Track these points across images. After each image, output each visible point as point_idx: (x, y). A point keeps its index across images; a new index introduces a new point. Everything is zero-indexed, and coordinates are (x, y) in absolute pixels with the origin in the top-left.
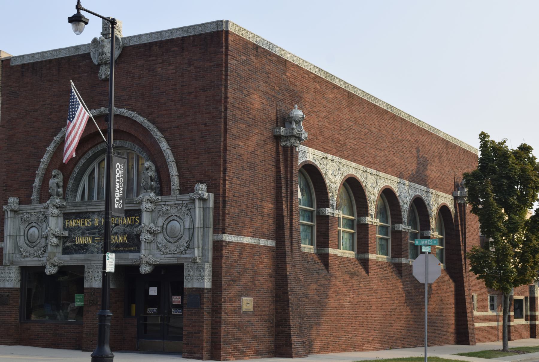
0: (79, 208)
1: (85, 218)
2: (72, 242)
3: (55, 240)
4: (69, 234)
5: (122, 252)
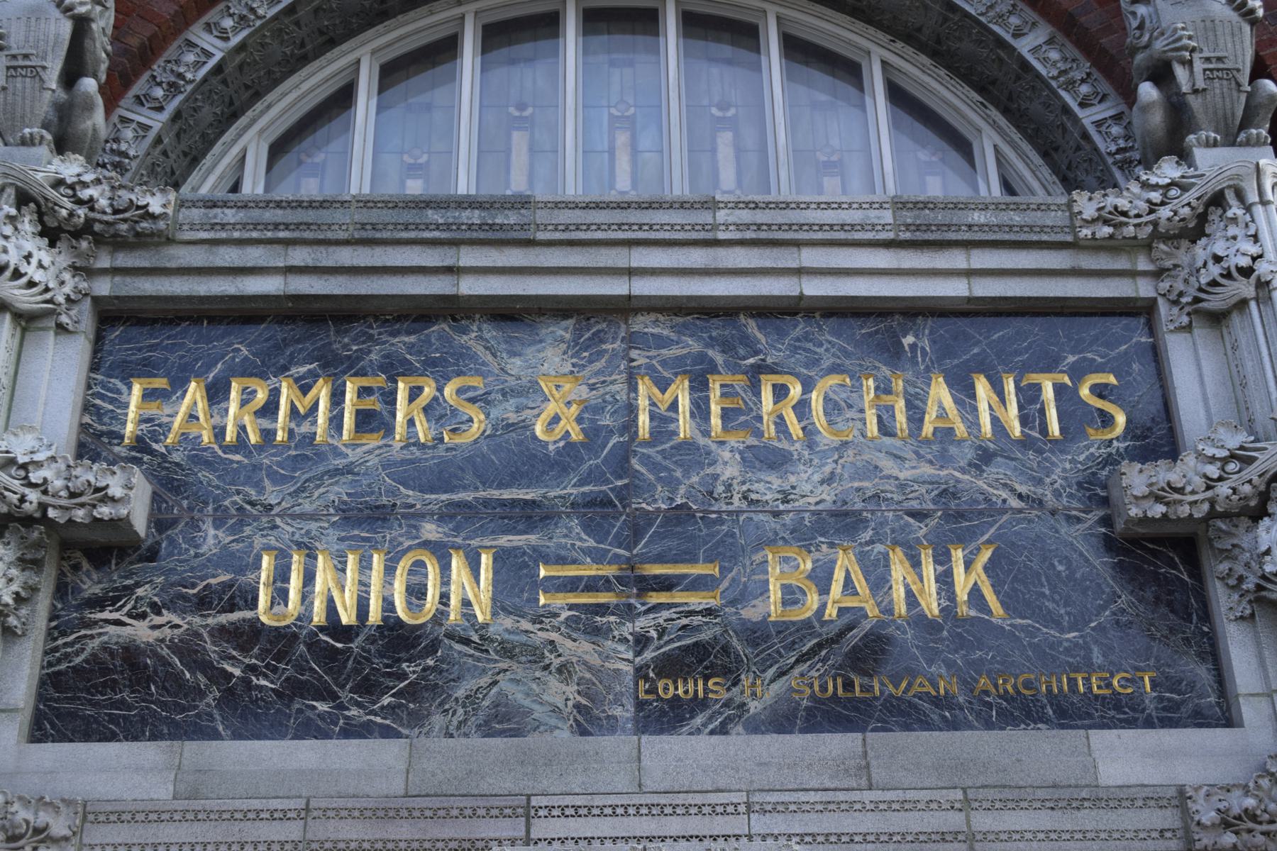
0: (346, 257)
1: (394, 368)
2: (203, 603)
4: (160, 523)
5: (954, 725)
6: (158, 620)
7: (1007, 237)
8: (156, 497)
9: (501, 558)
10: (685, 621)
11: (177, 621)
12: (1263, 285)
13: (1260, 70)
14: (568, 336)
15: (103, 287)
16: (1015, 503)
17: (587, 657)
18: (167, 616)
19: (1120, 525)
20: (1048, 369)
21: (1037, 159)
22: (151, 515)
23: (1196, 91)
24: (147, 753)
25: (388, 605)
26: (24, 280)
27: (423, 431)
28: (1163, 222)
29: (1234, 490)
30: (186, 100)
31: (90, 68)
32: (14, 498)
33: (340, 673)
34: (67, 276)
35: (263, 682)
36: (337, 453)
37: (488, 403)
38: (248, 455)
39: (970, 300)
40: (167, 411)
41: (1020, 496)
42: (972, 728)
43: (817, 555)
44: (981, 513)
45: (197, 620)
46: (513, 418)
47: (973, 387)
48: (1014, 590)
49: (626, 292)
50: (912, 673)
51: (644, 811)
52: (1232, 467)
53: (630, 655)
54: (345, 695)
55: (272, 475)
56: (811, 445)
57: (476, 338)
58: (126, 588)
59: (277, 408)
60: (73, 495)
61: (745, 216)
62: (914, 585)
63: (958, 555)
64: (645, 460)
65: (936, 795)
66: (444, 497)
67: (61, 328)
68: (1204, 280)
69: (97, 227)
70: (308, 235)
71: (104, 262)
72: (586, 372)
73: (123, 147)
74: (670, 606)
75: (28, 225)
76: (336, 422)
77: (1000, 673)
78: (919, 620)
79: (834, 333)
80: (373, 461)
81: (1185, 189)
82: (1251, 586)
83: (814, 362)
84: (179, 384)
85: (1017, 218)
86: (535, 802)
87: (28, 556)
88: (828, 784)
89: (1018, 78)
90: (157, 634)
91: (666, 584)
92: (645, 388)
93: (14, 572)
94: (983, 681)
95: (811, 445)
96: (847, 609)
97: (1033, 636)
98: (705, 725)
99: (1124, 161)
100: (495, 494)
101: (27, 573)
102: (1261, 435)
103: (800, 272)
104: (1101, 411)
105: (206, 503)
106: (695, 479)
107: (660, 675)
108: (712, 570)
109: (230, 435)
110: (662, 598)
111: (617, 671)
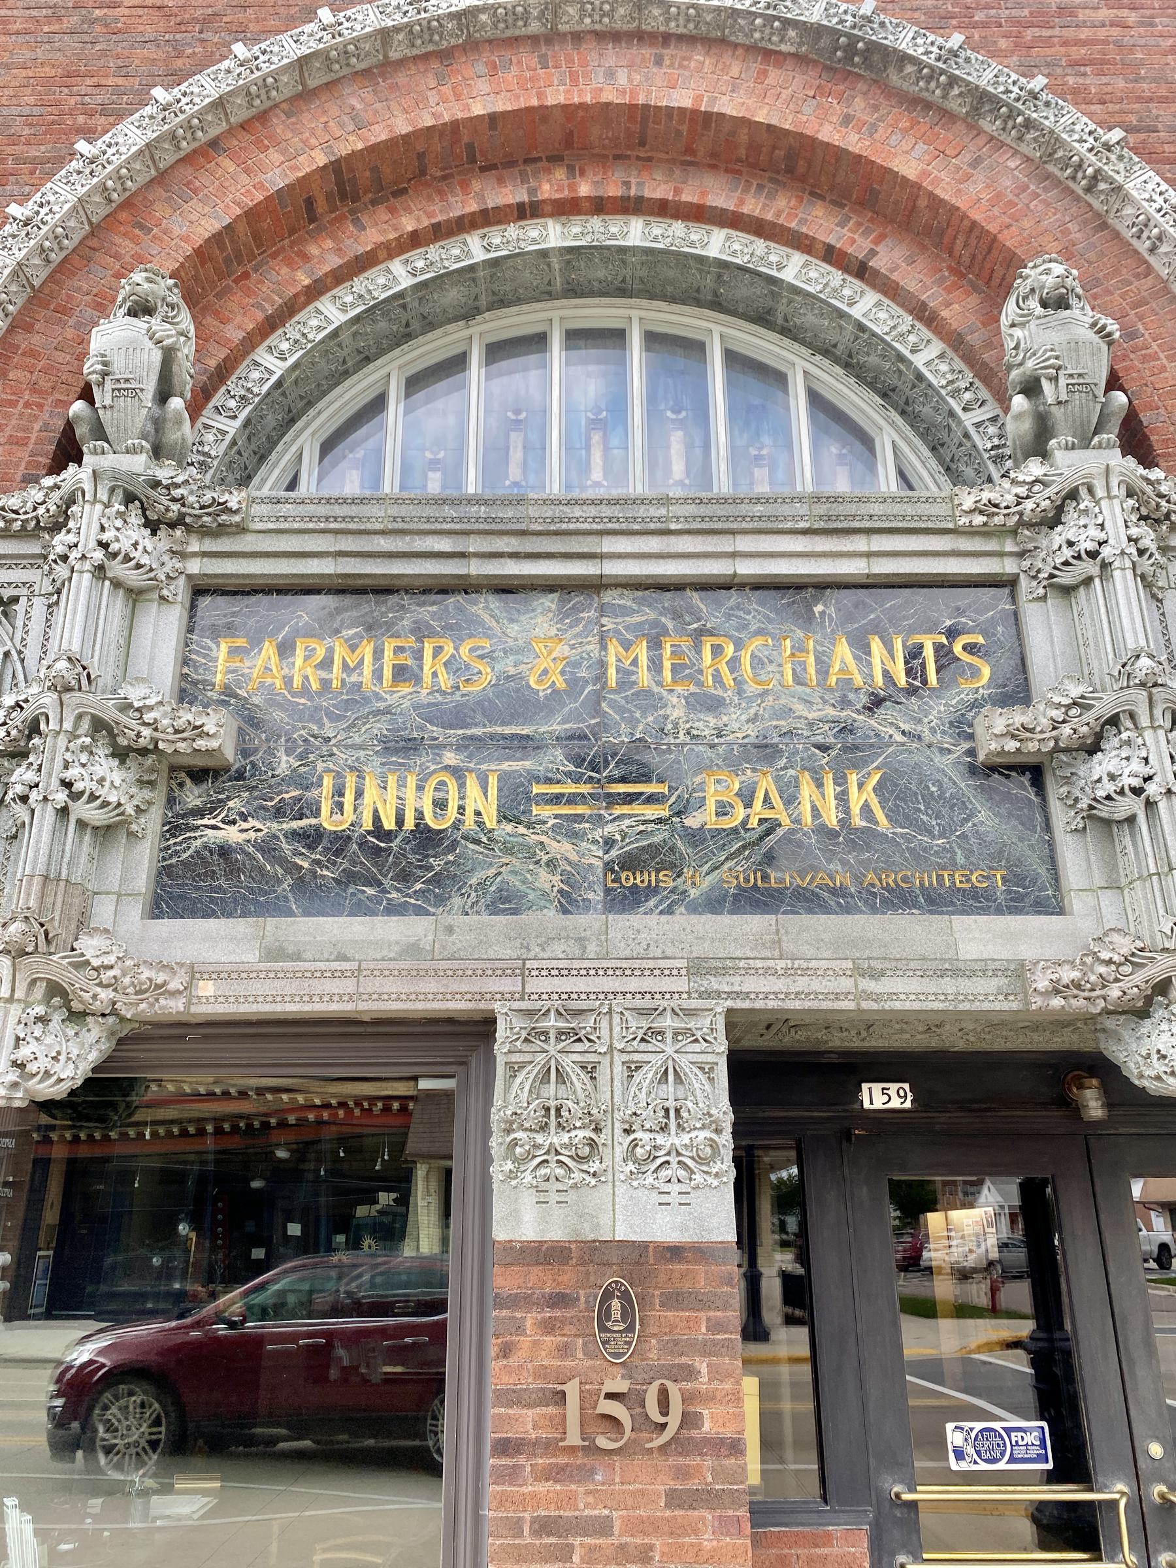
1: (421, 632)
2: (279, 813)
3: (110, 779)
4: (245, 753)
5: (847, 910)
6: (245, 826)
7: (900, 525)
8: (241, 731)
9: (504, 778)
10: (642, 828)
11: (259, 826)
12: (1105, 566)
13: (1114, 382)
14: (554, 606)
15: (194, 567)
16: (899, 738)
17: (568, 855)
18: (252, 822)
19: (981, 757)
20: (930, 631)
21: (926, 453)
22: (237, 745)
23: (1059, 403)
24: (239, 926)
25: (420, 815)
26: (133, 563)
27: (445, 680)
28: (1028, 512)
29: (1075, 731)
30: (255, 409)
31: (177, 389)
32: (132, 734)
33: (383, 866)
34: (166, 558)
35: (325, 872)
36: (379, 698)
37: (493, 659)
38: (311, 699)
39: (868, 576)
40: (248, 664)
41: (903, 733)
42: (861, 912)
43: (743, 778)
44: (872, 746)
45: (275, 825)
46: (512, 671)
47: (868, 645)
48: (897, 806)
49: (598, 572)
50: (815, 869)
51: (610, 972)
52: (1074, 712)
53: (600, 854)
54: (387, 882)
55: (329, 715)
56: (740, 692)
57: (485, 607)
58: (220, 801)
59: (332, 662)
60: (177, 732)
61: (691, 509)
62: (819, 803)
63: (853, 778)
64: (613, 704)
65: (832, 964)
66: (460, 732)
67: (162, 598)
68: (1058, 561)
69: (188, 520)
70: (352, 526)
71: (194, 546)
72: (568, 635)
73: (206, 449)
74: (631, 816)
75: (135, 519)
76: (378, 675)
77: (884, 870)
78: (823, 831)
79: (760, 603)
80: (406, 704)
81: (1046, 485)
82: (1085, 806)
83: (744, 627)
84: (256, 642)
85: (909, 509)
86: (529, 964)
87: (146, 778)
88: (749, 954)
89: (914, 386)
90: (245, 836)
91: (630, 798)
92: (614, 648)
93: (133, 790)
94: (871, 876)
95: (740, 692)
96: (766, 820)
97: (909, 841)
98: (656, 907)
99: (997, 456)
100: (499, 730)
101: (145, 791)
102: (1099, 687)
103: (734, 555)
104: (970, 665)
105: (279, 736)
106: (650, 719)
107: (622, 868)
108: (663, 789)
109: (297, 683)
110: (625, 810)
111: (590, 865)
